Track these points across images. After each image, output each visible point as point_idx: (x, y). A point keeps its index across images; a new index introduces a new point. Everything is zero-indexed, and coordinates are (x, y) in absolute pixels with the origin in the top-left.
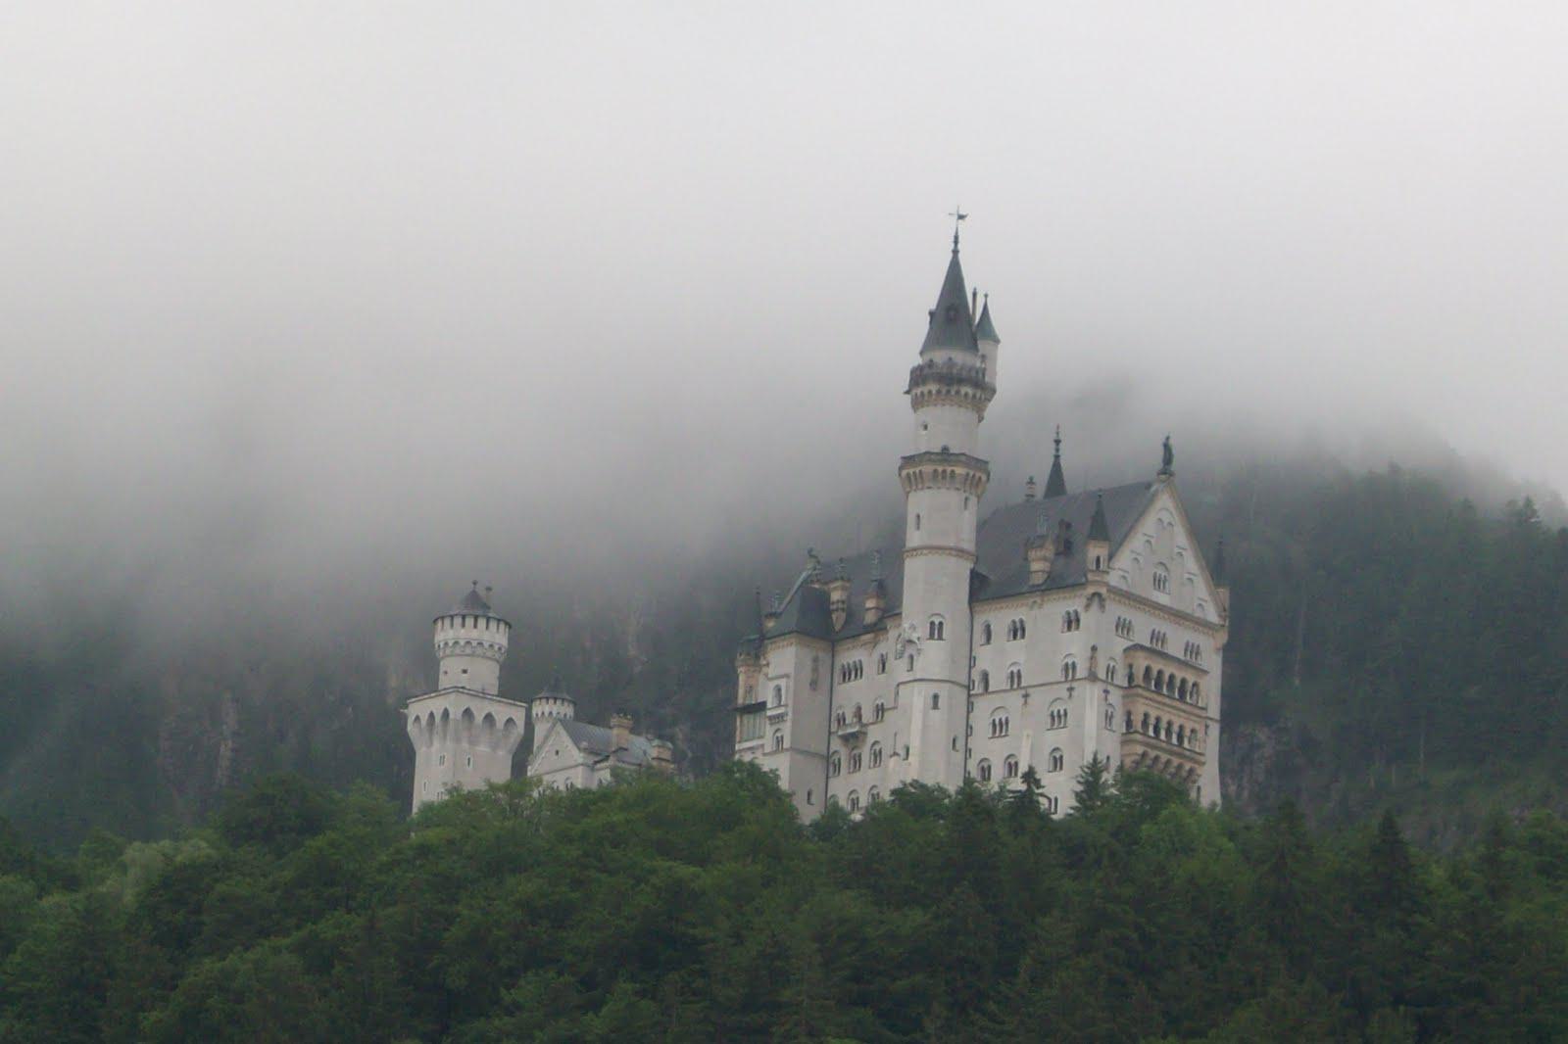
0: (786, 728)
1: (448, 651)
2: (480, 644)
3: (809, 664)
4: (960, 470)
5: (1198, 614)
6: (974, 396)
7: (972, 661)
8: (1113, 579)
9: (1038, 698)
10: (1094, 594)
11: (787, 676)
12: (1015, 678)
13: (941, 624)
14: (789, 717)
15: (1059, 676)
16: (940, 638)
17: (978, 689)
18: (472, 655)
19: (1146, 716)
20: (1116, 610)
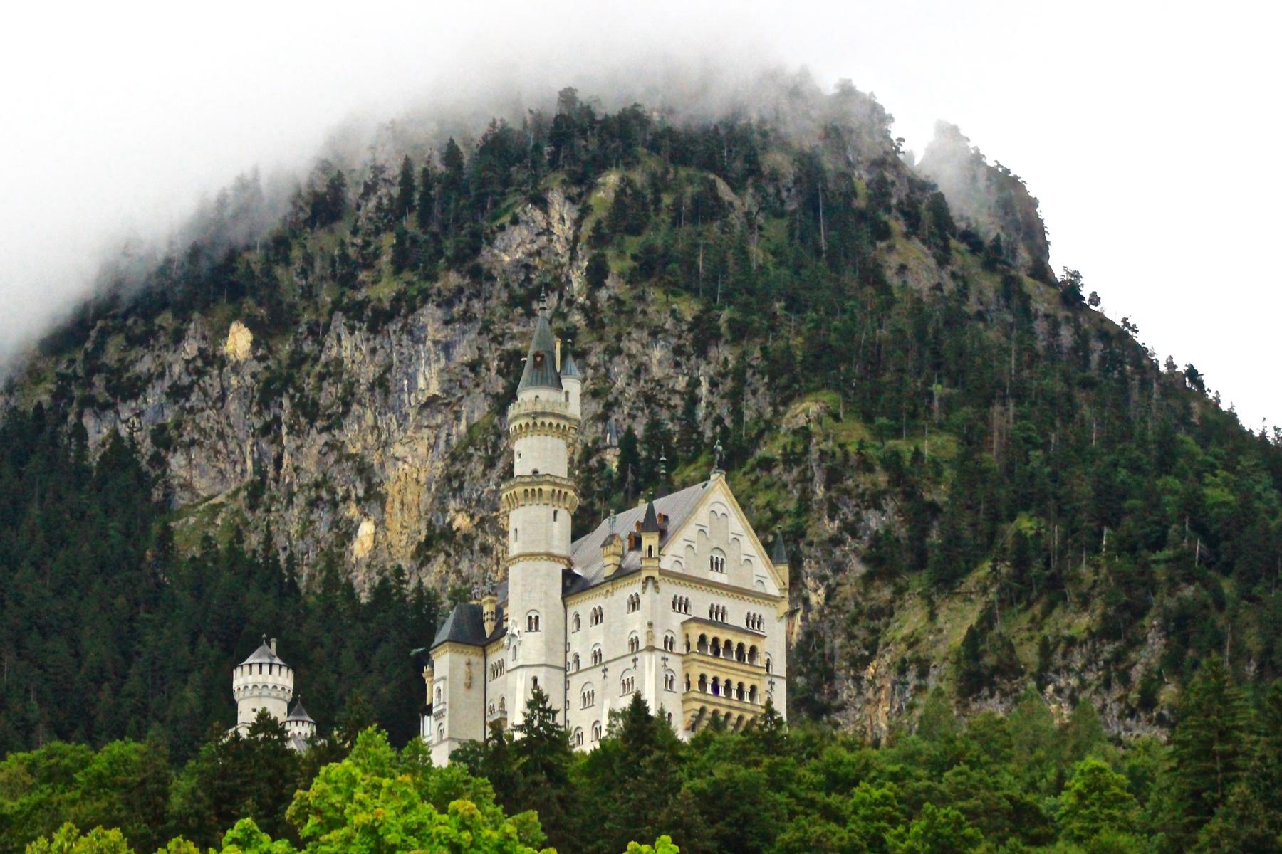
0: (445, 721)
1: (241, 694)
2: (265, 686)
3: (463, 668)
4: (546, 488)
5: (759, 589)
6: (558, 425)
7: (567, 644)
8: (666, 564)
9: (615, 671)
10: (647, 578)
11: (444, 678)
12: (597, 656)
13: (537, 618)
14: (446, 714)
15: (627, 650)
16: (537, 629)
17: (571, 670)
18: (260, 696)
19: (703, 677)
20: (670, 590)
